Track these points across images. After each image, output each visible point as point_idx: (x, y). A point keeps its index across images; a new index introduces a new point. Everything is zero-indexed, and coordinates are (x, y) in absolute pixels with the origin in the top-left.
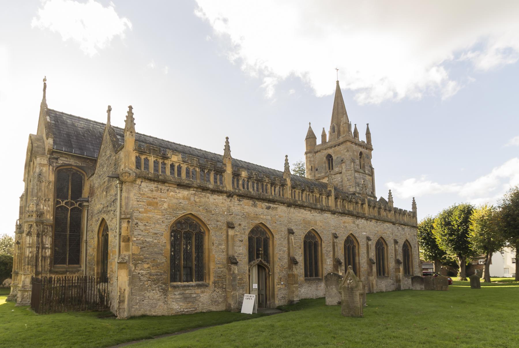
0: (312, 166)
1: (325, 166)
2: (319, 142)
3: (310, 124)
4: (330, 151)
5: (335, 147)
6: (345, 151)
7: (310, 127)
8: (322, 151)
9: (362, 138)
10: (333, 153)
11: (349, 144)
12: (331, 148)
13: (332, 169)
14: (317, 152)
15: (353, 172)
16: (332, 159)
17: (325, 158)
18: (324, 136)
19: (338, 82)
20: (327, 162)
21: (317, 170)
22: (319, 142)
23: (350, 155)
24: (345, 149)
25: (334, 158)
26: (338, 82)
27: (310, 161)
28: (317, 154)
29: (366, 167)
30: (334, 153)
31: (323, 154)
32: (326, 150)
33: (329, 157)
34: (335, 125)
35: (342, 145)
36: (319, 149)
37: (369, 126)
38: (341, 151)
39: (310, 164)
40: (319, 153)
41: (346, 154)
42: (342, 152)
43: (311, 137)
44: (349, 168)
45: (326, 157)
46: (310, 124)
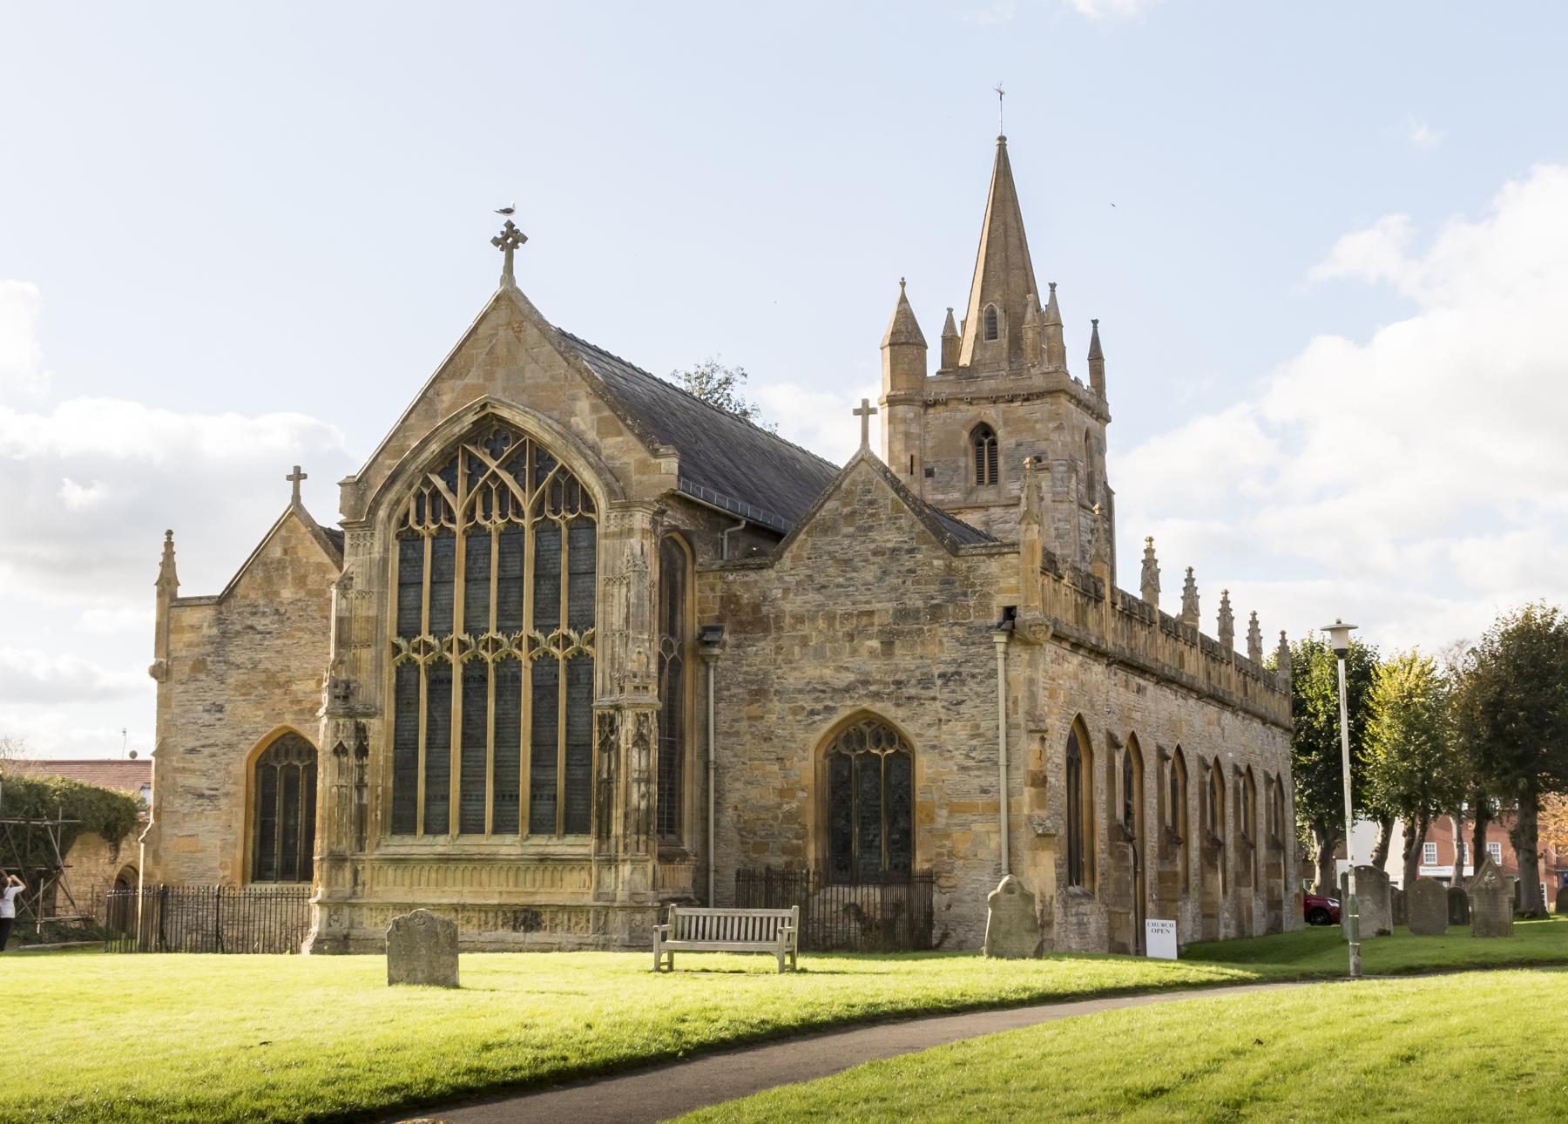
0: (912, 457)
1: (966, 467)
2: (933, 365)
3: (903, 284)
4: (991, 414)
5: (1012, 401)
6: (1051, 425)
7: (904, 300)
8: (953, 404)
9: (1077, 368)
10: (1001, 423)
11: (1063, 399)
12: (995, 402)
13: (994, 480)
14: (935, 403)
15: (1075, 506)
16: (994, 443)
17: (965, 435)
18: (951, 342)
19: (1002, 139)
20: (971, 451)
21: (929, 473)
22: (933, 365)
23: (1065, 445)
24: (1051, 419)
25: (1005, 440)
26: (1002, 139)
27: (907, 435)
28: (931, 411)
29: (1098, 488)
30: (1006, 423)
31: (958, 416)
32: (971, 404)
33: (983, 434)
34: (999, 312)
35: (1038, 402)
36: (944, 396)
37: (1099, 330)
38: (1036, 422)
39: (907, 449)
40: (940, 408)
41: (1054, 436)
42: (1038, 426)
43: (905, 339)
44: (1064, 492)
45: (972, 434)
46: (903, 284)
